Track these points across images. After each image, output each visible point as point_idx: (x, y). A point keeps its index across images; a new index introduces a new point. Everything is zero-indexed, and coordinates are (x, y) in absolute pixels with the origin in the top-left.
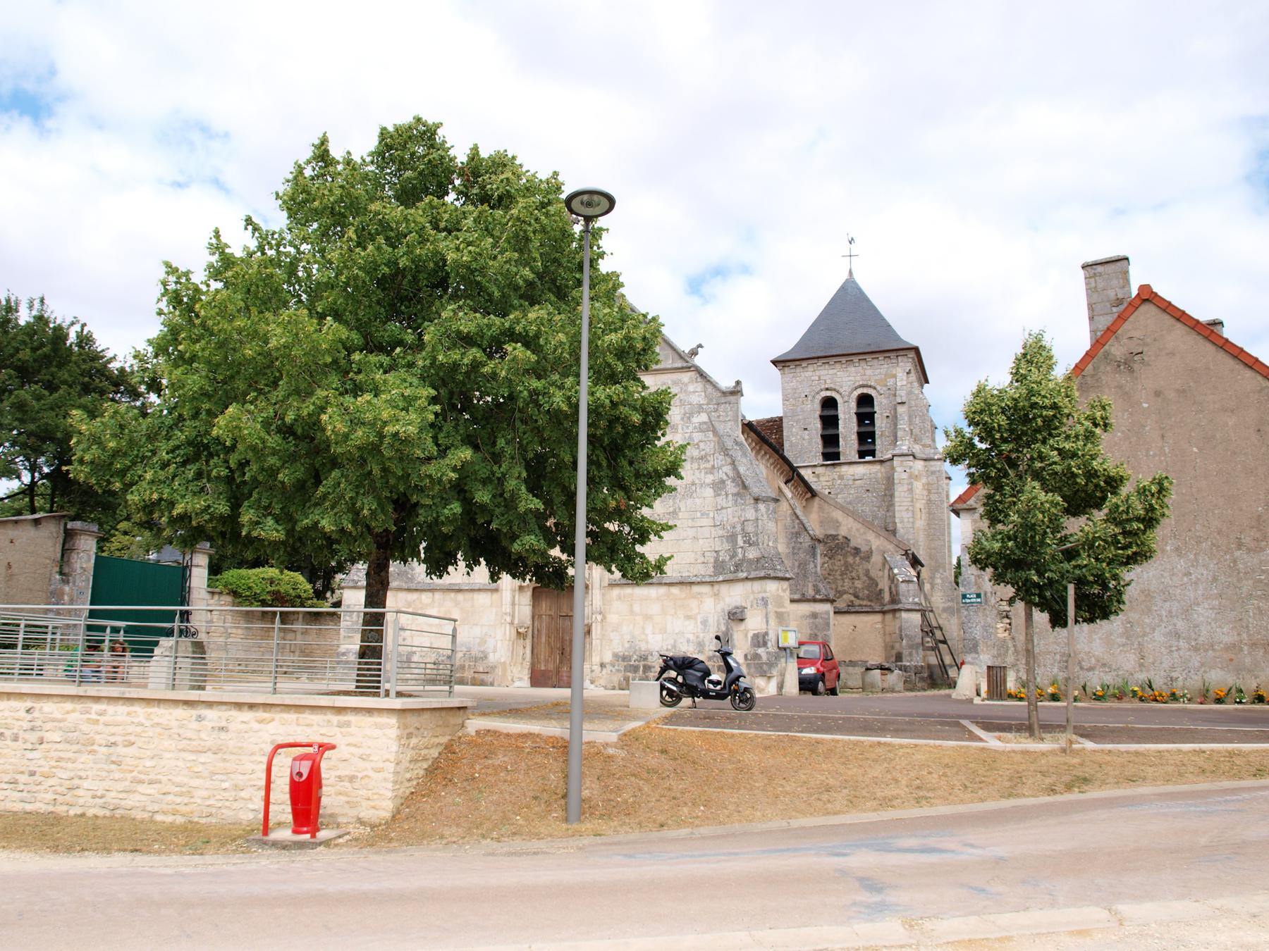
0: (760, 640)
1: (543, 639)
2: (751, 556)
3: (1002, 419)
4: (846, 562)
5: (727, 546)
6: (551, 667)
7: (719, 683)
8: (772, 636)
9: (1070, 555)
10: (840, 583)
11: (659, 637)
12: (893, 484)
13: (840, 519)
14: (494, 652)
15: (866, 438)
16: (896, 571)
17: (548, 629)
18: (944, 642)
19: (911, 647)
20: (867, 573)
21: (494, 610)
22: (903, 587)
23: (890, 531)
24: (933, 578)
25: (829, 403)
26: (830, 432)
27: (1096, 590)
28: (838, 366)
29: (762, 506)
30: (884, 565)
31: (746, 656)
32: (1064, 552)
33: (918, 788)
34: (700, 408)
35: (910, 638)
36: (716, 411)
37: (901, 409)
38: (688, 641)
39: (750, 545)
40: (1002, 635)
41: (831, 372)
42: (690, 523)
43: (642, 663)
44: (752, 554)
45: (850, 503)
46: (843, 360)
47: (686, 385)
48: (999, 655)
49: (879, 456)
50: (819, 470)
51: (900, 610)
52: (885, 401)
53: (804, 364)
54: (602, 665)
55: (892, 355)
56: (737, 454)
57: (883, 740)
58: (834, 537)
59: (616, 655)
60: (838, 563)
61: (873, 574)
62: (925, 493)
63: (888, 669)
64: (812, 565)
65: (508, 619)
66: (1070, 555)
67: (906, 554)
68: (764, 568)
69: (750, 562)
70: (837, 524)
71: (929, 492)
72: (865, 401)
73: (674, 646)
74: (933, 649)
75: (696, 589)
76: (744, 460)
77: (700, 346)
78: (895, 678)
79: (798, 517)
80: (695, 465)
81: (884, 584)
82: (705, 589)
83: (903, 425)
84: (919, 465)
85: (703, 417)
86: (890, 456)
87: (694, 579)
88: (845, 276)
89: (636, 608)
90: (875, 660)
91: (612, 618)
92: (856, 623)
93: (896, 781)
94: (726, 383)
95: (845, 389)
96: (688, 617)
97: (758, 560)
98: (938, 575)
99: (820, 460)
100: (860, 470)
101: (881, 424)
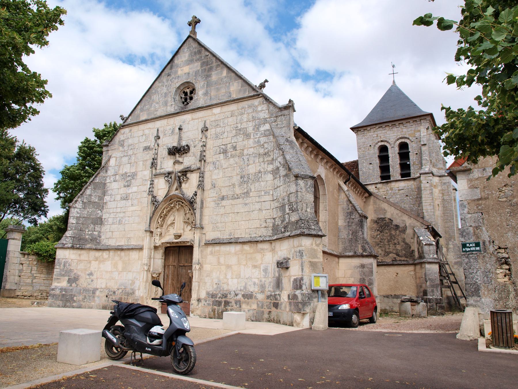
0: (298, 284)
4: (391, 234)
5: (280, 214)
8: (306, 280)
10: (387, 247)
11: (235, 281)
12: (421, 190)
13: (386, 208)
14: (139, 289)
16: (421, 238)
18: (456, 283)
19: (433, 286)
20: (404, 240)
22: (426, 248)
23: (419, 216)
24: (447, 244)
25: (383, 149)
28: (387, 128)
29: (301, 182)
30: (414, 235)
31: (289, 295)
34: (265, 121)
36: (275, 121)
37: (423, 148)
38: (254, 284)
39: (293, 211)
40: (502, 280)
41: (383, 132)
42: (257, 199)
44: (294, 218)
45: (397, 203)
46: (390, 124)
47: (257, 107)
49: (412, 176)
50: (379, 186)
51: (424, 263)
53: (369, 128)
54: (199, 300)
55: (417, 119)
56: (287, 147)
58: (383, 219)
60: (386, 235)
61: (408, 240)
62: (441, 195)
64: (360, 233)
65: (146, 268)
67: (428, 228)
70: (385, 211)
71: (443, 194)
72: (404, 146)
73: (245, 288)
74: (449, 287)
75: (260, 246)
76: (291, 151)
77: (266, 81)
78: (421, 307)
79: (351, 202)
81: (415, 247)
82: (266, 246)
83: (425, 157)
84: (436, 180)
85: (267, 127)
88: (391, 84)
89: (222, 260)
91: (207, 267)
92: (398, 271)
94: (281, 102)
95: (392, 141)
96: (255, 267)
97: (297, 222)
98: (450, 243)
99: (379, 180)
100: (402, 184)
101: (413, 157)
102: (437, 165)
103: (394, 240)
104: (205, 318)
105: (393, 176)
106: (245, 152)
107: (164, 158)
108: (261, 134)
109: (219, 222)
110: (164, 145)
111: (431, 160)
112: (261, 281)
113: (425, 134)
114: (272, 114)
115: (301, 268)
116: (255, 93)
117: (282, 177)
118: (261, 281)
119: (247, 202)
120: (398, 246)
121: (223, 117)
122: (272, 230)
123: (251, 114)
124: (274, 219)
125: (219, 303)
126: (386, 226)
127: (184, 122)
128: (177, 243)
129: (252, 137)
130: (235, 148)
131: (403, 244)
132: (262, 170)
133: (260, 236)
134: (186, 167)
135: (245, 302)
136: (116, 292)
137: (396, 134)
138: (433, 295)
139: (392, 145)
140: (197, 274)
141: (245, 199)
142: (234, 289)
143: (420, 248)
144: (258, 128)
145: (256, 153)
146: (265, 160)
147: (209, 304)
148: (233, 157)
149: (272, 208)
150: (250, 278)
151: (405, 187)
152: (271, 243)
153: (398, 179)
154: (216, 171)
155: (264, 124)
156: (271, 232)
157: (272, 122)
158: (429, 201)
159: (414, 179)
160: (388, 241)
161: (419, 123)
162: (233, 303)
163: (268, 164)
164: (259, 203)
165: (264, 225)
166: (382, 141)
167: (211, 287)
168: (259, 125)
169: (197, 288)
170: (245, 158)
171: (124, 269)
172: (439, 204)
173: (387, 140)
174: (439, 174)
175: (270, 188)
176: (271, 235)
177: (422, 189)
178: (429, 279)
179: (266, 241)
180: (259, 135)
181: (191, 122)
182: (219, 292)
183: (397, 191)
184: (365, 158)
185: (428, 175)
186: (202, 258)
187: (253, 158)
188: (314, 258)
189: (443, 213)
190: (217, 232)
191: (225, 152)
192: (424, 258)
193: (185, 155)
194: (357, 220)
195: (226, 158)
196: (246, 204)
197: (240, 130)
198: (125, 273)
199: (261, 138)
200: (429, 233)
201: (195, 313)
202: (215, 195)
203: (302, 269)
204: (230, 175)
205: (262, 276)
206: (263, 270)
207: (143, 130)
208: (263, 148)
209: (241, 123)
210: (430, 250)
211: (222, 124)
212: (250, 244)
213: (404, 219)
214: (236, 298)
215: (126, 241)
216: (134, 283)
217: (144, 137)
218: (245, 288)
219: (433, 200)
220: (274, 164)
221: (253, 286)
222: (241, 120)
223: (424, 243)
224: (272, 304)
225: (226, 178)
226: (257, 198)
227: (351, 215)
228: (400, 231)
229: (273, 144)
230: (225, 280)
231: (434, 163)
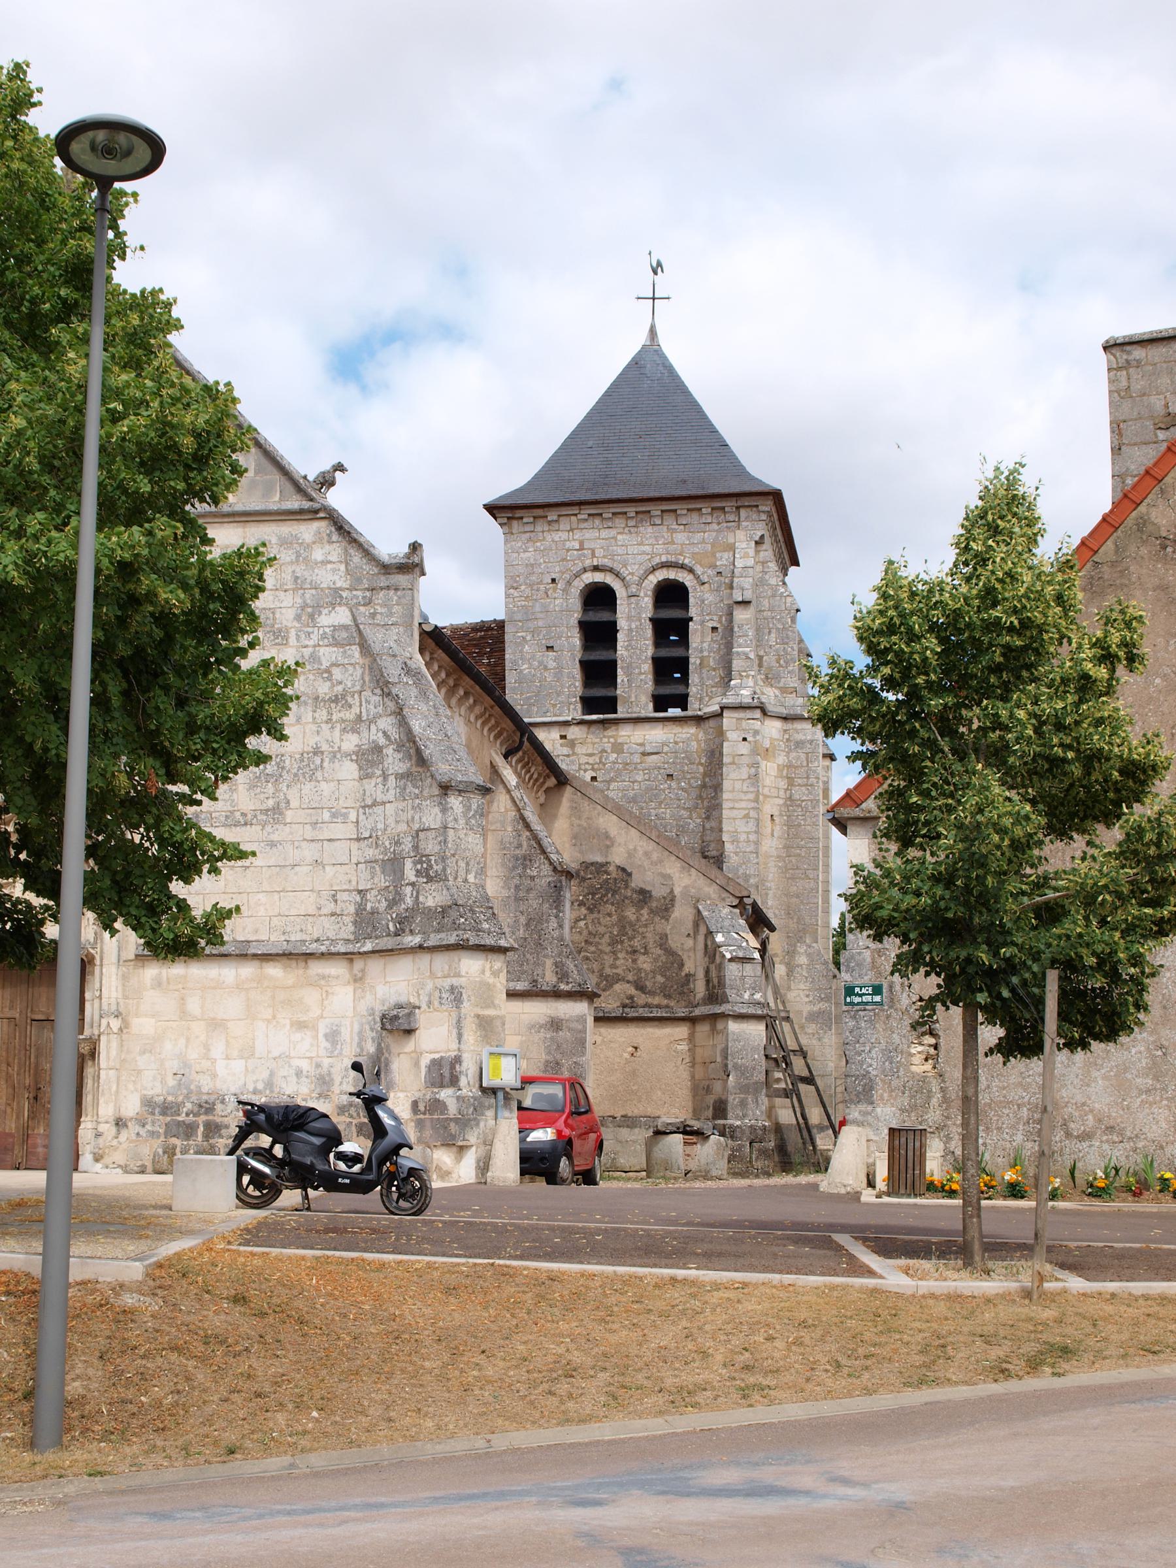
0: (444, 1073)
2: (430, 903)
3: (932, 643)
4: (622, 918)
5: (382, 881)
7: (356, 1158)
8: (468, 1067)
9: (1050, 914)
10: (608, 960)
11: (238, 1065)
12: (720, 764)
13: (613, 832)
15: (671, 670)
16: (719, 938)
18: (810, 1080)
23: (712, 856)
24: (791, 953)
25: (599, 598)
26: (600, 655)
27: (1098, 982)
28: (620, 522)
29: (455, 802)
30: (696, 925)
31: (415, 1104)
32: (1038, 910)
33: (747, 1368)
34: (335, 598)
35: (742, 1070)
36: (368, 603)
37: (740, 615)
39: (430, 879)
40: (920, 1067)
41: (605, 534)
42: (309, 833)
44: (433, 898)
45: (634, 800)
46: (631, 510)
47: (308, 547)
48: (913, 1107)
50: (574, 732)
51: (724, 1016)
52: (710, 598)
53: (552, 516)
54: (120, 1123)
55: (728, 504)
56: (408, 692)
57: (680, 1273)
58: (600, 868)
59: (148, 1103)
60: (607, 920)
61: (674, 943)
62: (783, 784)
63: (699, 1133)
64: (553, 924)
66: (1050, 914)
67: (741, 904)
68: (456, 927)
69: (429, 913)
71: (791, 782)
72: (671, 595)
73: (269, 1084)
74: (786, 1094)
75: (317, 968)
76: (423, 708)
77: (339, 467)
78: (711, 1151)
79: (527, 826)
80: (322, 714)
81: (694, 964)
82: (336, 969)
83: (744, 647)
84: (773, 728)
85: (342, 616)
86: (716, 708)
87: (313, 947)
89: (194, 1005)
90: (676, 1111)
91: (143, 1025)
92: (638, 1041)
93: (705, 1354)
94: (391, 548)
95: (632, 571)
96: (300, 1026)
97: (444, 911)
98: (801, 949)
99: (575, 712)
100: (656, 735)
101: (701, 644)
102: (778, 677)
103: (630, 939)
104: (143, 1172)
105: (626, 701)
108: (324, 636)
111: (760, 658)
112: (318, 1066)
113: (751, 562)
114: (359, 580)
115: (455, 1032)
116: (306, 505)
117: (392, 779)
118: (318, 1066)
119: (275, 837)
120: (642, 958)
122: (355, 923)
123: (290, 569)
124: (360, 892)
126: (607, 891)
129: (292, 640)
131: (659, 952)
132: (325, 747)
133: (317, 940)
137: (648, 549)
138: (744, 1116)
139: (633, 589)
140: (114, 1044)
141: (268, 828)
142: (233, 1090)
143: (712, 967)
146: (334, 718)
147: (152, 1134)
149: (354, 860)
150: (285, 1058)
151: (664, 744)
152: (351, 960)
153: (643, 714)
155: (333, 605)
156: (351, 928)
157: (359, 604)
158: (743, 805)
159: (699, 720)
160: (613, 942)
161: (731, 517)
163: (344, 730)
164: (313, 845)
165: (330, 907)
166: (596, 569)
167: (158, 1084)
168: (317, 608)
169: (114, 1088)
172: (776, 813)
173: (617, 567)
174: (784, 712)
175: (350, 803)
176: (352, 937)
177: (726, 760)
178: (736, 1066)
179: (338, 954)
180: (315, 637)
182: (187, 1097)
183: (637, 758)
184: (531, 625)
185: (749, 714)
186: (126, 997)
188: (488, 1007)
189: (786, 847)
192: (724, 1000)
194: (544, 882)
199: (322, 650)
200: (742, 922)
201: (107, 1160)
203: (460, 1036)
205: (322, 1052)
206: (326, 1035)
208: (329, 679)
210: (743, 978)
212: (285, 960)
213: (669, 871)
219: (756, 800)
220: (365, 734)
221: (294, 1079)
223: (728, 956)
224: (354, 1129)
226: (308, 827)
227: (525, 867)
228: (651, 911)
229: (359, 671)
230: (206, 1064)
231: (770, 668)
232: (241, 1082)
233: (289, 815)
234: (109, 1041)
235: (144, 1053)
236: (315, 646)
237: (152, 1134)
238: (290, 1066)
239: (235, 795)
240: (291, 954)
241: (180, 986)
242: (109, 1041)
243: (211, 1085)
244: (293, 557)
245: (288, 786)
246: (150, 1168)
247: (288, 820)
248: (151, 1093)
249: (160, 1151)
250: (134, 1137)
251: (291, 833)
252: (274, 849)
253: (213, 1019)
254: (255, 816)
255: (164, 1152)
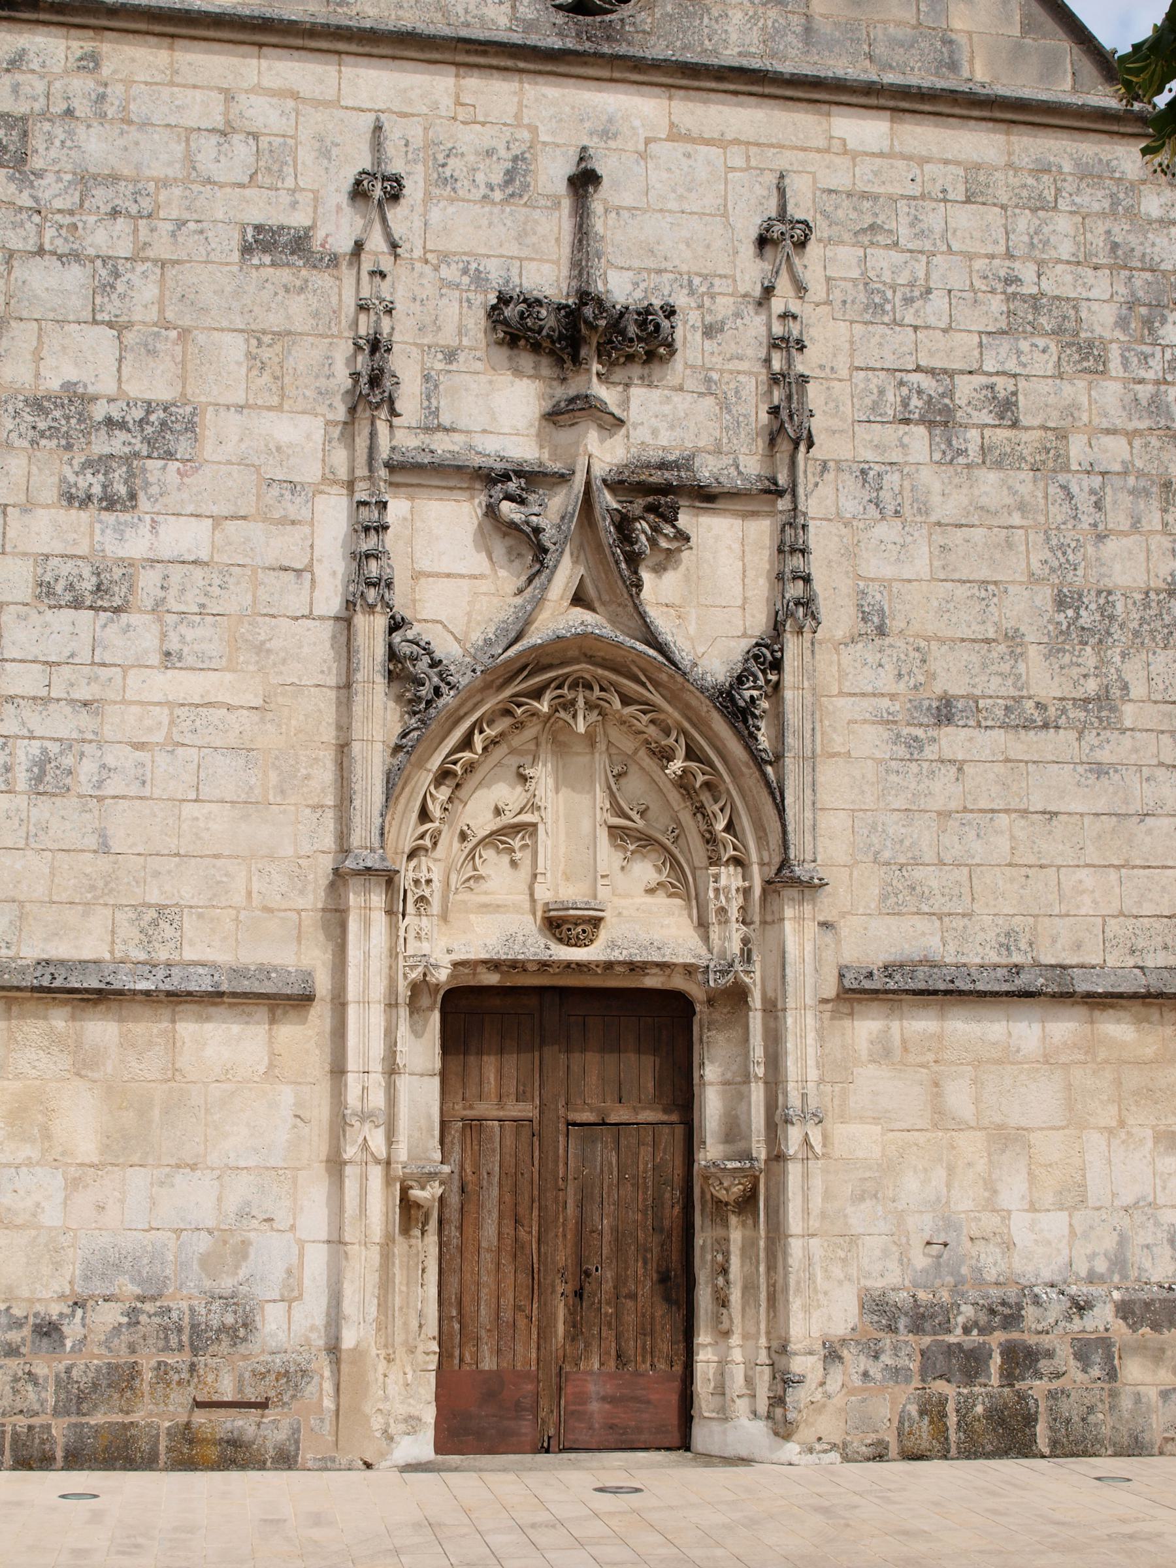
1: (490, 1231)
6: (526, 1355)
11: (1055, 1223)
14: (291, 1297)
17: (512, 1179)
21: (287, 1096)
43: (998, 1338)
47: (1133, 188)
54: (832, 1355)
59: (879, 1308)
73: (1119, 1262)
104: (880, 1457)
106: (1077, 449)
107: (451, 356)
109: (929, 856)
110: (445, 257)
121: (916, 190)
125: (970, 1364)
127: (606, 134)
128: (569, 967)
129: (1115, 366)
130: (1006, 410)
134: (654, 456)
135: (1141, 1349)
136: (72, 1331)
141: (1090, 737)
142: (1047, 1275)
144: (1148, 323)
145: (1140, 474)
147: (896, 1373)
148: (998, 465)
150: (1146, 1206)
154: (888, 531)
162: (1065, 1357)
167: (893, 1265)
170: (1080, 486)
171: (123, 1148)
181: (663, 150)
187: (1126, 500)
190: (921, 924)
191: (940, 418)
193: (636, 370)
195: (952, 456)
196: (1100, 770)
197: (1035, 302)
198: (138, 1179)
201: (806, 1434)
202: (886, 681)
204: (984, 573)
207: (229, 96)
209: (1040, 263)
211: (904, 232)
212: (1136, 1007)
214: (1077, 1324)
215: (128, 931)
216: (242, 1251)
217: (242, 150)
218: (1119, 1262)
222: (1038, 241)
225: (961, 591)
230: (990, 1222)
232: (1062, 1260)
233: (1129, 714)
234: (806, 1175)
235: (862, 1199)
236: (1157, 382)
237: (896, 1373)
238: (1157, 1224)
239: (1022, 667)
240: (1161, 995)
241: (930, 1057)
242: (806, 1175)
243: (1003, 1266)
244: (1106, 204)
245: (1123, 655)
246: (894, 1449)
247: (1128, 723)
248: (879, 1284)
249: (913, 1409)
250: (857, 1381)
251: (1136, 750)
252: (1104, 780)
253: (1000, 1127)
254: (1064, 711)
255: (922, 1413)
